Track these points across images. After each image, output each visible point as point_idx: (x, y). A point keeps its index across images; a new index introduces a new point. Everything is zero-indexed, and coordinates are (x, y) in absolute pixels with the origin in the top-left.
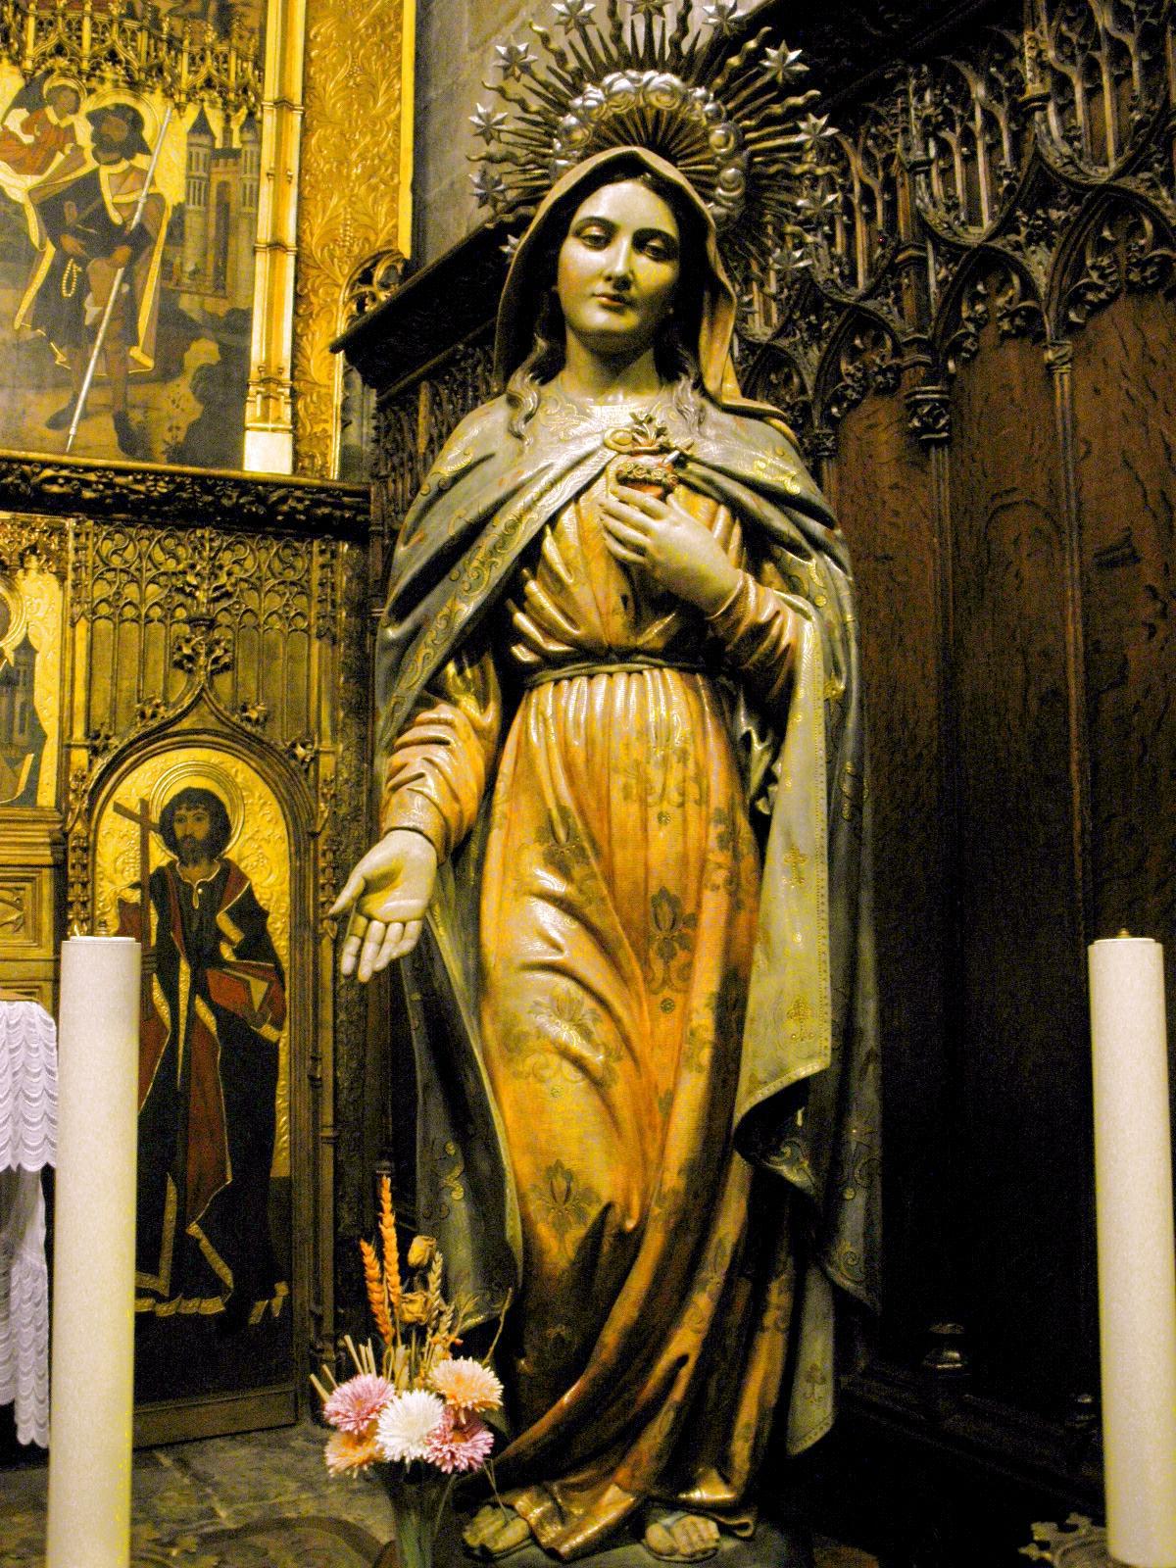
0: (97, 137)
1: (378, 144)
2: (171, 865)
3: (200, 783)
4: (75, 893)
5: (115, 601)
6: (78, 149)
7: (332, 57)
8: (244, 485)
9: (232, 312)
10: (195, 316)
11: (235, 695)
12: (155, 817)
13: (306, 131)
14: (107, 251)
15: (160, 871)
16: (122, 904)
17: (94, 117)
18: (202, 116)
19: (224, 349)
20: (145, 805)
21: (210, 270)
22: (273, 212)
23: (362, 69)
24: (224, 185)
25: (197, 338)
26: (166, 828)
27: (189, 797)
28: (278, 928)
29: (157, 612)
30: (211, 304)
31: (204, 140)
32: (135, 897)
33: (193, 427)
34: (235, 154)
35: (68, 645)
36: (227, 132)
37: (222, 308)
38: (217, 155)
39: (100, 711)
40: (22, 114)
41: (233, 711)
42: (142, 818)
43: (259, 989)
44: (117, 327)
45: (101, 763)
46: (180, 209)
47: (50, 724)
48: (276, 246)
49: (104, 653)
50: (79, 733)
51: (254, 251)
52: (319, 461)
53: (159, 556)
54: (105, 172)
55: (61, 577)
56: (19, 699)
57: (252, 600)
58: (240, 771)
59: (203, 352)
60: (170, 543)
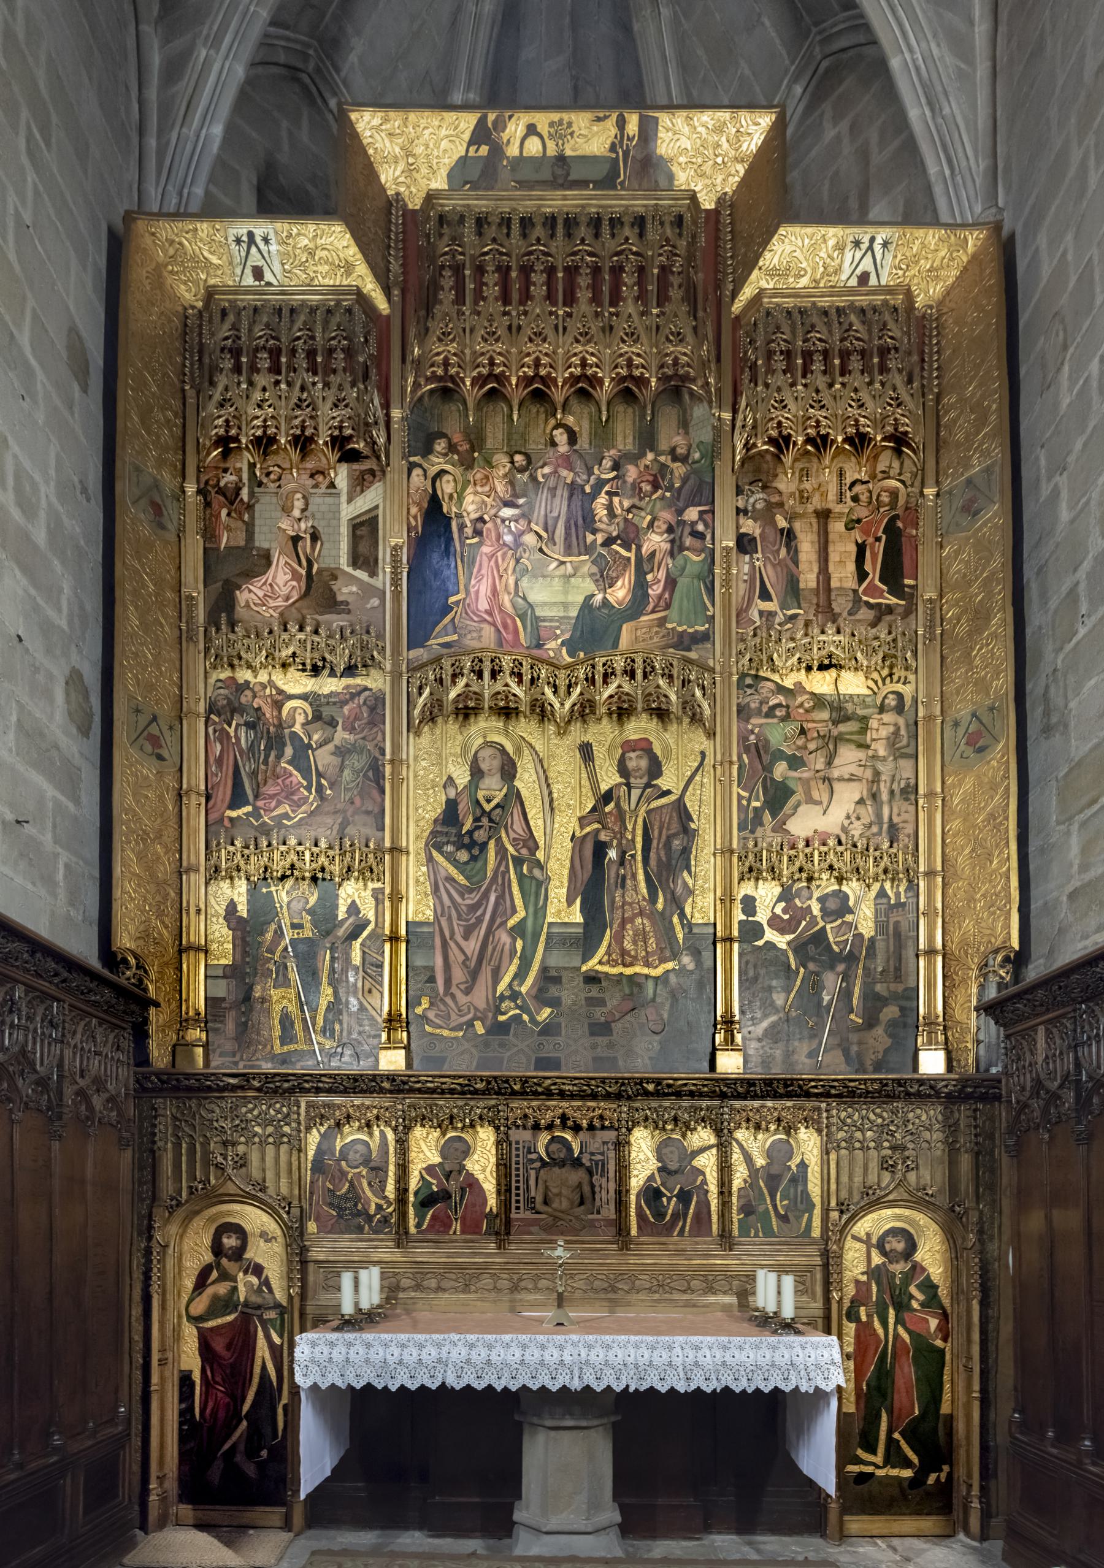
0: (822, 910)
1: (994, 887)
2: (884, 1264)
3: (898, 1224)
4: (835, 1277)
5: (850, 1140)
6: (814, 917)
7: (960, 841)
8: (921, 1082)
9: (906, 989)
10: (885, 994)
11: (918, 1183)
12: (874, 1241)
13: (944, 885)
14: (832, 968)
15: (877, 1266)
16: (857, 1282)
17: (818, 899)
18: (882, 888)
19: (902, 1009)
20: (868, 1235)
21: (892, 969)
22: (929, 933)
23: (981, 845)
24: (897, 924)
25: (886, 1005)
26: (881, 1246)
27: (893, 1232)
28: (943, 1293)
29: (872, 1144)
30: (892, 986)
31: (884, 900)
32: (864, 1278)
33: (886, 1051)
34: (903, 905)
35: (825, 1163)
36: (898, 894)
37: (900, 988)
38: (891, 908)
39: (844, 1194)
40: (783, 904)
41: (918, 1190)
42: (867, 1241)
43: (934, 1323)
44: (841, 1004)
45: (845, 1217)
46: (872, 940)
47: (817, 1200)
48: (931, 952)
49: (845, 1163)
50: (833, 1203)
51: (917, 956)
52: (963, 1063)
53: (872, 1116)
54: (828, 926)
55: (819, 1131)
56: (800, 1189)
57: (927, 1135)
58: (921, 1218)
59: (891, 1012)
60: (878, 1111)
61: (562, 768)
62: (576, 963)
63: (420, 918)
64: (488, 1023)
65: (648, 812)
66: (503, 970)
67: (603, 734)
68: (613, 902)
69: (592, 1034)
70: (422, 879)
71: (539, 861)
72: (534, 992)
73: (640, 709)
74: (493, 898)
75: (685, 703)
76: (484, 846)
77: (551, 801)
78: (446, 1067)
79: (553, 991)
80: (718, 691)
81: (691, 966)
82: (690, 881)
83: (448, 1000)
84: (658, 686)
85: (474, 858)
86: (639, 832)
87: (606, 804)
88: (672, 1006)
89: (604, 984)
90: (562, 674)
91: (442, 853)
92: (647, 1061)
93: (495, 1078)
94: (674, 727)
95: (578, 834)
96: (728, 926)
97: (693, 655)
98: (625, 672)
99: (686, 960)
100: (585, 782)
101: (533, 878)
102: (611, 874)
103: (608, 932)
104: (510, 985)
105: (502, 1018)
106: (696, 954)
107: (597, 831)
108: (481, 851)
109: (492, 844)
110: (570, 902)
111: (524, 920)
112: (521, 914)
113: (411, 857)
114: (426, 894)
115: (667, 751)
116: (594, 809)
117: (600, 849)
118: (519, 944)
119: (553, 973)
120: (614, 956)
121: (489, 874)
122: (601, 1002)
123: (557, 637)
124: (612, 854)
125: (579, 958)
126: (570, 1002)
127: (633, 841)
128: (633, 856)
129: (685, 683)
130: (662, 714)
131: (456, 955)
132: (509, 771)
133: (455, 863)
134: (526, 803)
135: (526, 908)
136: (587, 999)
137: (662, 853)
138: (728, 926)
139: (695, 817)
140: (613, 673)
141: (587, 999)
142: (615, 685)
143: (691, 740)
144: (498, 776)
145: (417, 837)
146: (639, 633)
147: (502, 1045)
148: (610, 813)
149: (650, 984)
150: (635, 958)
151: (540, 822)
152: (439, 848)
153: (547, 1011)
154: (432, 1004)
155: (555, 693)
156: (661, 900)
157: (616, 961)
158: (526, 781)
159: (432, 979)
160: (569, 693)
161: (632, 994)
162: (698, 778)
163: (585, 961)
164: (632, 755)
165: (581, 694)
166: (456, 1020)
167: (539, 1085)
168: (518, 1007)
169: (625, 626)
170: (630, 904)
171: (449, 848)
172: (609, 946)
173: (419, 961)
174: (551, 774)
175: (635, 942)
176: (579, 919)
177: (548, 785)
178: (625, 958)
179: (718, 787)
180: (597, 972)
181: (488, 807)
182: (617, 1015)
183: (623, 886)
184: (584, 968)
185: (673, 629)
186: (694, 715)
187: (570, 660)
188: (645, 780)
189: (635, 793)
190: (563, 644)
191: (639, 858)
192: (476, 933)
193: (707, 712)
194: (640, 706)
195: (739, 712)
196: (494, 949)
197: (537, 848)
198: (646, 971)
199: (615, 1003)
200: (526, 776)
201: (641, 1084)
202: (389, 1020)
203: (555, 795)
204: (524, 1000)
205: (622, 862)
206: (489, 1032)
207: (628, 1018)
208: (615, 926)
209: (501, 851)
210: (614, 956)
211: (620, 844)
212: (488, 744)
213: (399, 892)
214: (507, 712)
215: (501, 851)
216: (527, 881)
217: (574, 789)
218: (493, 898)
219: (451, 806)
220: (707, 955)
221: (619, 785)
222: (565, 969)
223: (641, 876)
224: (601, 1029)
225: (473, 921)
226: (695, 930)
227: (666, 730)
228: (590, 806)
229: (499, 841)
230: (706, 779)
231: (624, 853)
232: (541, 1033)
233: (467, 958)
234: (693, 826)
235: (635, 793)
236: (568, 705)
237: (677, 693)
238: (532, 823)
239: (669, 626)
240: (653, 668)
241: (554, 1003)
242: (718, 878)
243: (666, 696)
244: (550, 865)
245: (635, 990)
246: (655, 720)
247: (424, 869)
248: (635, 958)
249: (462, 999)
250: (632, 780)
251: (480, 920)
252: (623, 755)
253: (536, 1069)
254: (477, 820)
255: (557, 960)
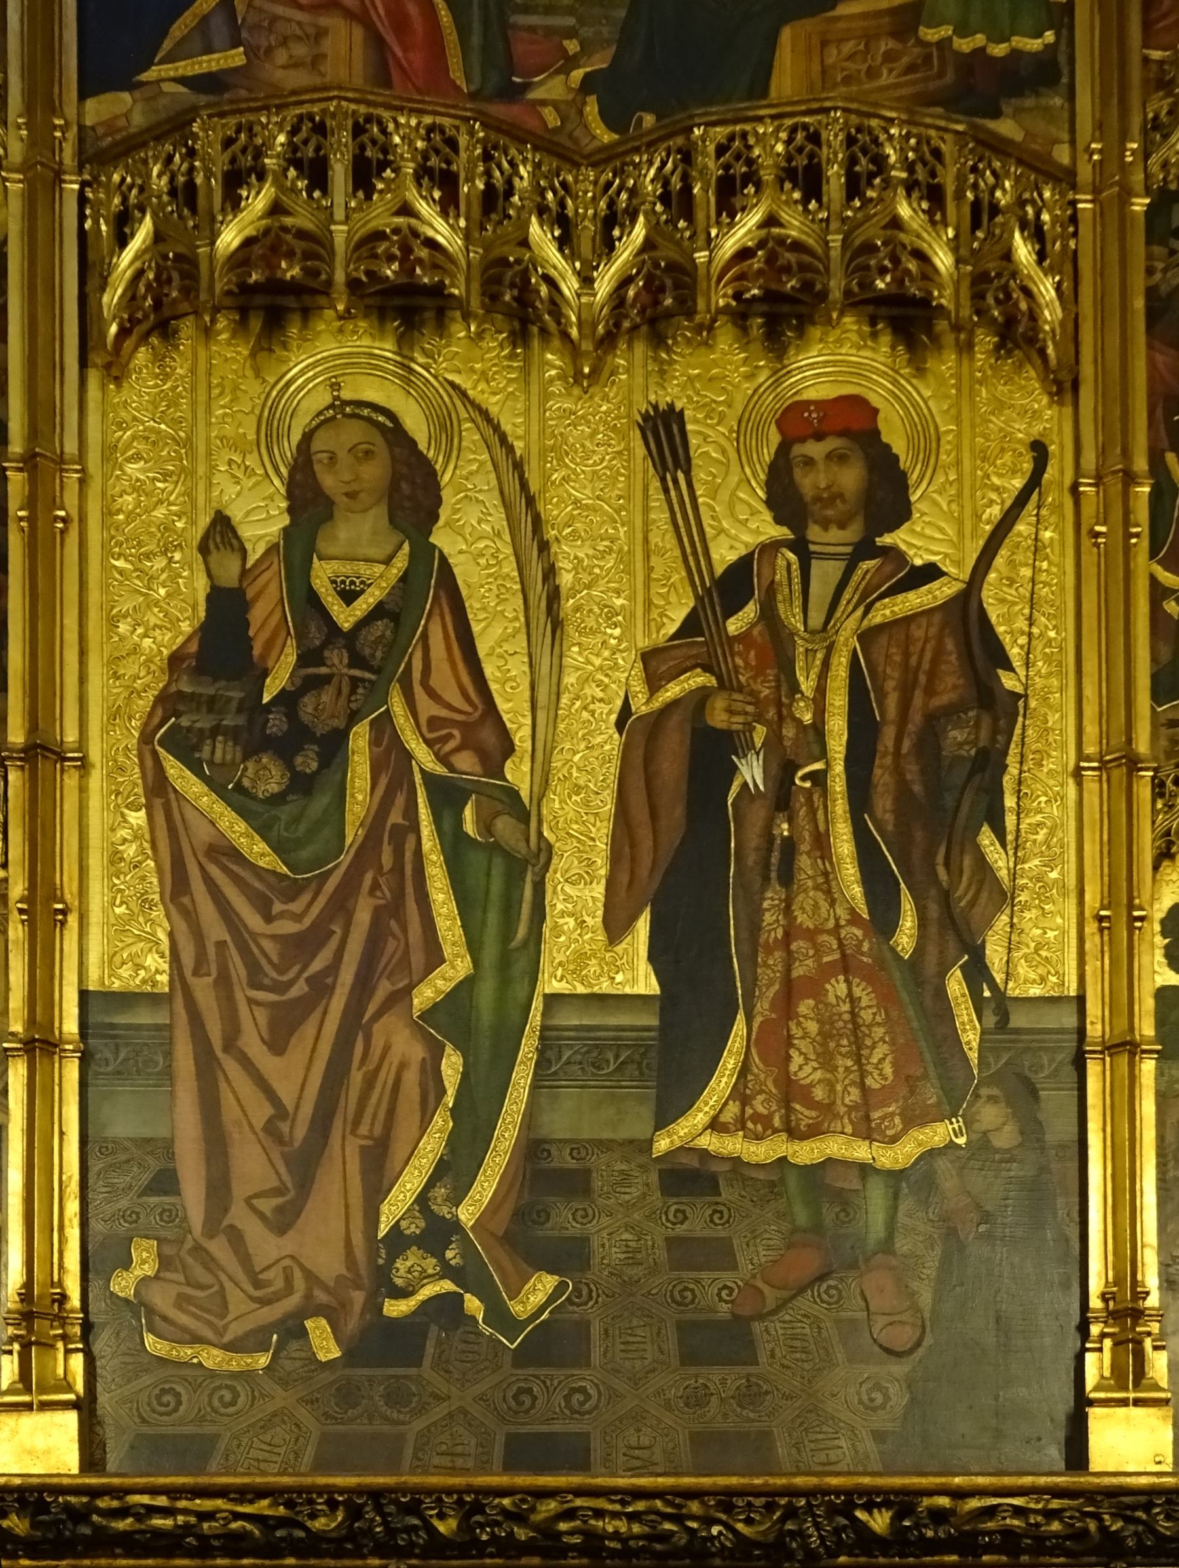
61: (584, 496)
62: (636, 1125)
63: (124, 980)
64: (352, 1324)
65: (867, 637)
66: (399, 1149)
67: (720, 384)
68: (754, 926)
69: (690, 1357)
70: (131, 851)
71: (513, 794)
72: (500, 1224)
73: (836, 294)
74: (363, 916)
75: (980, 281)
76: (334, 747)
77: (554, 596)
78: (213, 1466)
79: (564, 1219)
80: (1086, 244)
81: (1006, 1137)
82: (999, 859)
83: (219, 1248)
84: (896, 223)
85: (301, 785)
86: (838, 701)
87: (730, 611)
88: (945, 1262)
89: (727, 1194)
90: (586, 182)
91: (195, 767)
92: (869, 1445)
93: (376, 1495)
94: (946, 364)
95: (641, 706)
96: (1122, 1002)
97: (1006, 127)
98: (788, 174)
99: (990, 1115)
100: (663, 538)
101: (496, 848)
102: (743, 841)
103: (740, 1026)
104: (422, 1200)
105: (395, 1308)
106: (1023, 1093)
107: (701, 697)
108: (325, 763)
109: (360, 739)
110: (616, 926)
111: (467, 986)
112: (457, 966)
113: (95, 780)
114: (145, 903)
115: (927, 441)
116: (691, 626)
117: (713, 754)
118: (452, 1066)
119: (564, 1160)
120: (759, 1105)
121: (352, 834)
122: (719, 1255)
123: (571, 62)
124: (752, 771)
125: (647, 1113)
126: (617, 1255)
127: (818, 729)
128: (819, 779)
129: (982, 212)
130: (908, 319)
131: (243, 1103)
132: (414, 496)
133: (240, 799)
134: (472, 606)
135: (474, 946)
136: (672, 1243)
137: (912, 771)
138: (1122, 1002)
139: (1015, 653)
140: (747, 179)
141: (672, 1243)
142: (754, 218)
143: (1000, 406)
144: (380, 513)
145: (114, 715)
146: (832, 55)
147: (395, 1397)
148: (744, 637)
149: (876, 1198)
150: (827, 1109)
151: (518, 668)
152: (185, 747)
153: (540, 1288)
154: (165, 1262)
155: (563, 243)
156: (908, 922)
157: (766, 1121)
158: (471, 534)
159: (166, 1182)
160: (608, 246)
161: (817, 1227)
162: (1021, 527)
163: (665, 1117)
164: (815, 449)
165: (648, 245)
166: (243, 1314)
167: (519, 1517)
168: (447, 1271)
169: (786, 34)
170: (811, 935)
171: (222, 750)
172: (744, 1070)
173: (123, 1123)
174: (550, 510)
175: (826, 1060)
176: (646, 983)
177: (544, 547)
178: (795, 1111)
179: (1090, 558)
180: (704, 1154)
181: (345, 617)
182: (771, 1296)
183: (787, 877)
184: (662, 1144)
185: (944, 45)
186: (1010, 321)
187: (607, 137)
188: (853, 533)
189: (825, 574)
190: (588, 85)
191: (838, 783)
192: (309, 1028)
193: (1051, 314)
194: (836, 286)
195: (1153, 315)
196: (370, 1082)
197: (508, 749)
198: (861, 1152)
199: (763, 1255)
200: (471, 516)
201: (847, 1510)
202: (27, 1316)
203: (566, 579)
204: (467, 1248)
205: (782, 796)
206: (352, 1355)
207: (804, 1303)
208: (763, 1007)
209: (391, 759)
210: (759, 1105)
211: (774, 742)
212: (343, 410)
213: (54, 894)
214: (408, 304)
215: (391, 759)
216: (476, 860)
217: (626, 559)
218: (363, 916)
219: (226, 609)
220: (1055, 1101)
221: (770, 548)
222: (604, 1145)
223: (844, 845)
224: (718, 1341)
225: (299, 989)
226: (1018, 1020)
227: (920, 372)
228: (678, 616)
229: (384, 728)
230: (1047, 530)
231: (789, 768)
232: (522, 1357)
233: (280, 1112)
234: (1009, 682)
235: (825, 574)
236: (604, 285)
237: (955, 246)
238: (489, 670)
239: (931, 35)
240: (880, 161)
241: (567, 1257)
242: (1091, 849)
243: (922, 257)
244: (553, 804)
245: (829, 1214)
246: (886, 339)
247: (138, 818)
248: (827, 1109)
249: (266, 1247)
250: (814, 532)
251: (321, 987)
252: (784, 449)
253: (509, 1467)
254: (307, 658)
255: (576, 1117)
